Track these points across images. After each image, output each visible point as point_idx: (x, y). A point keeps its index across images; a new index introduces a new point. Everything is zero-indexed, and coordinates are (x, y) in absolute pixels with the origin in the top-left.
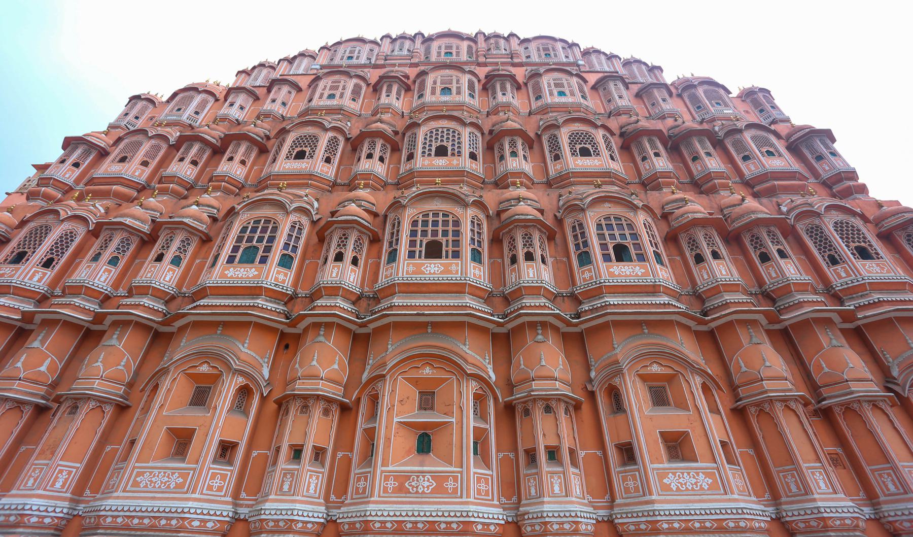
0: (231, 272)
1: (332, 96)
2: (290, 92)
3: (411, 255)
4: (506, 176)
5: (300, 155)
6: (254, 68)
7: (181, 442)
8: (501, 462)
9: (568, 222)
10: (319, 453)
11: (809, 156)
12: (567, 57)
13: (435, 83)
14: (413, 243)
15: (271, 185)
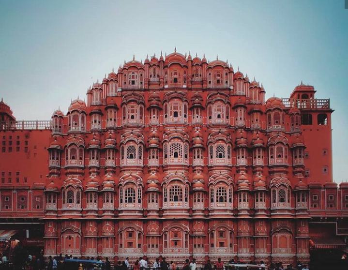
0: (127, 205)
1: (133, 117)
2: (115, 112)
3: (171, 200)
4: (195, 167)
5: (131, 157)
6: (93, 89)
7: (130, 245)
8: (190, 246)
9: (210, 187)
10: (157, 245)
11: (294, 155)
12: (227, 82)
13: (171, 109)
14: (171, 197)
15: (127, 170)
